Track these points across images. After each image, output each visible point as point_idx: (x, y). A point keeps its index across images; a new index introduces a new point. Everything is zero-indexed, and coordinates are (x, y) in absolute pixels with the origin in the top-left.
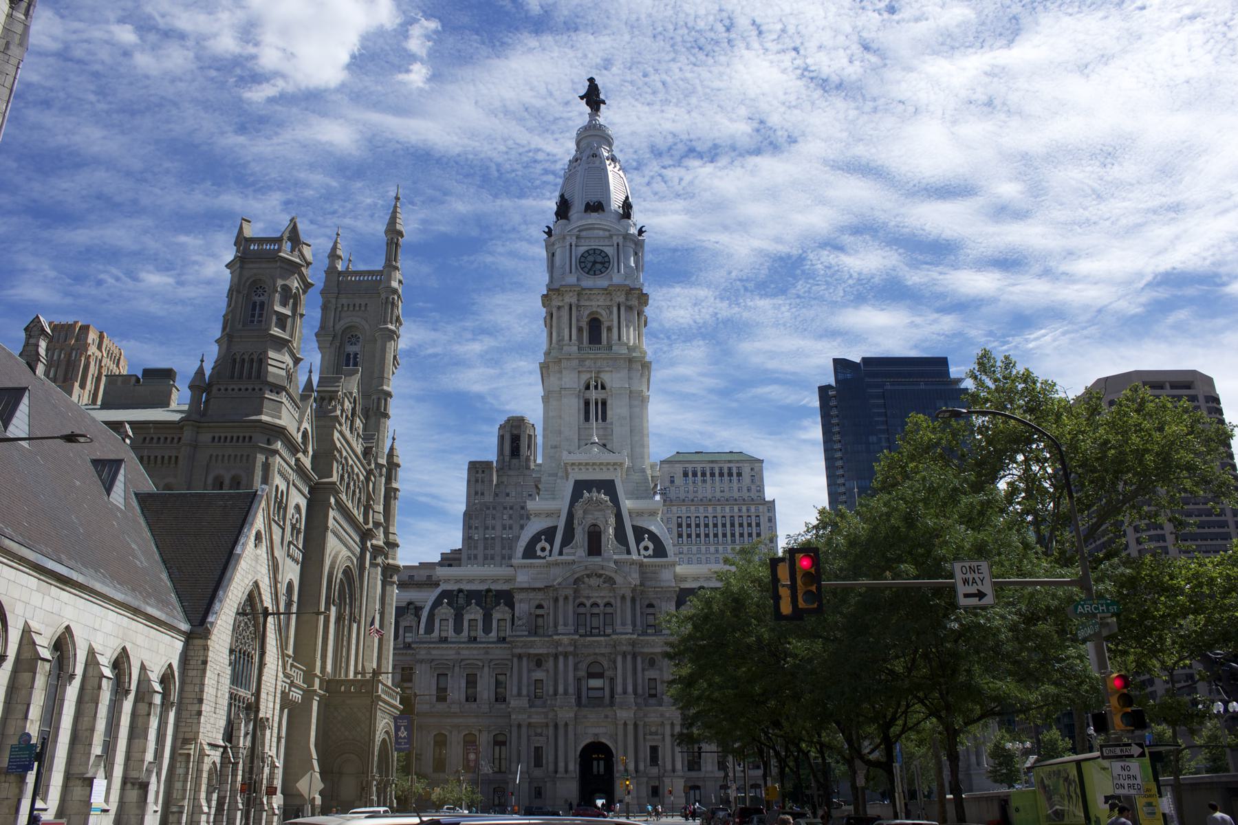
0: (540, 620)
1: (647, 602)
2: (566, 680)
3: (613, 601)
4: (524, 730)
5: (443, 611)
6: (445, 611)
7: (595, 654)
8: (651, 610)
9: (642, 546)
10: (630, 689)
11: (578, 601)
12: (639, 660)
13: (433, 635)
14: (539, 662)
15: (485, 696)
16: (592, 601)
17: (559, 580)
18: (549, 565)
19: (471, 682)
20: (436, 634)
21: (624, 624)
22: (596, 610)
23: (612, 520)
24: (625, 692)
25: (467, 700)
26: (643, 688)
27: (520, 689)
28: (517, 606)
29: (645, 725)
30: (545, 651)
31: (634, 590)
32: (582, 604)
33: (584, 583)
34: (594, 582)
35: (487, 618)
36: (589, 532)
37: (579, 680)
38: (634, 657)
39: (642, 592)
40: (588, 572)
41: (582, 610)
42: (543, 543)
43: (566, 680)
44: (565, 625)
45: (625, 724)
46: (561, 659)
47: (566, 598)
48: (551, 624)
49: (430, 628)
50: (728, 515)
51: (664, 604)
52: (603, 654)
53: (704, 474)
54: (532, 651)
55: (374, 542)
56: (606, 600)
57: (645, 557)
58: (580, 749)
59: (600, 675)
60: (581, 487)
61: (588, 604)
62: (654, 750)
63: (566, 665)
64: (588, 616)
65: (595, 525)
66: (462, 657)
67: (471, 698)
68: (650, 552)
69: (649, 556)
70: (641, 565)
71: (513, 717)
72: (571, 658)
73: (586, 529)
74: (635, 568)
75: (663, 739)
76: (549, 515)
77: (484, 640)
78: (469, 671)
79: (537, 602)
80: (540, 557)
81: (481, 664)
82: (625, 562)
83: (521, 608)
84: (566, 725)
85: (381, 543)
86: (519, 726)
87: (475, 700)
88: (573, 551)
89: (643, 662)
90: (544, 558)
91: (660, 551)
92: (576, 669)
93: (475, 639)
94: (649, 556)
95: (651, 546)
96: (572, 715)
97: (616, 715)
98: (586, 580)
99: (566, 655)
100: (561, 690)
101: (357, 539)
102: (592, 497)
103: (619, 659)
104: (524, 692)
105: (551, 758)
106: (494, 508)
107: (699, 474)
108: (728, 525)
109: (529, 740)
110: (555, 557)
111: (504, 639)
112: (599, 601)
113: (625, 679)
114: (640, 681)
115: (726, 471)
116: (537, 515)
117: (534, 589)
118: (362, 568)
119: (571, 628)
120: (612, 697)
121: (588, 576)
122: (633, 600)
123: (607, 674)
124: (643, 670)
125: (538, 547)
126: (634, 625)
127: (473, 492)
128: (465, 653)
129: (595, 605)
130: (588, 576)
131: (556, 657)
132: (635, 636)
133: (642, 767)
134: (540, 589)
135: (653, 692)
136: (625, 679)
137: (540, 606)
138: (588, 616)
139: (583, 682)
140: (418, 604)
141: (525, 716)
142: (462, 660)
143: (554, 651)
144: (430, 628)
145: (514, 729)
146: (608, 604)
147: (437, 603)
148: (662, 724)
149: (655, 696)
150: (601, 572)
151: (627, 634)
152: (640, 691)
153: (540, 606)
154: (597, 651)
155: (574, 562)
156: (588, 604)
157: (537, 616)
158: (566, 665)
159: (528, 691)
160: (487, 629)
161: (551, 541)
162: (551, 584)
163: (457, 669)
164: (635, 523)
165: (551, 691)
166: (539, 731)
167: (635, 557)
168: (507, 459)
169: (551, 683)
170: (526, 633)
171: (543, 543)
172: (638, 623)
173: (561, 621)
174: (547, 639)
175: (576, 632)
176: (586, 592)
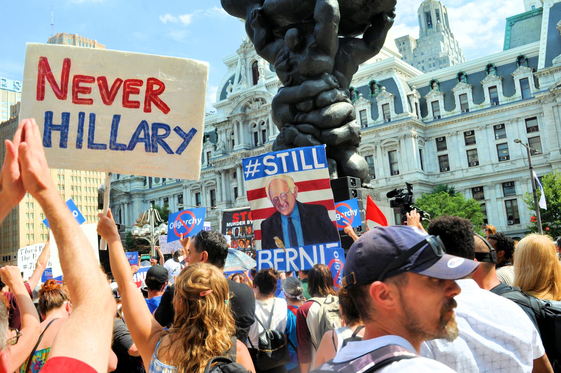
16: (259, 120)
33: (250, 108)
34: (255, 105)
36: (253, 68)
47: (238, 124)
54: (226, 167)
98: (250, 105)
104: (224, 198)
125: (228, 90)
161: (232, 83)
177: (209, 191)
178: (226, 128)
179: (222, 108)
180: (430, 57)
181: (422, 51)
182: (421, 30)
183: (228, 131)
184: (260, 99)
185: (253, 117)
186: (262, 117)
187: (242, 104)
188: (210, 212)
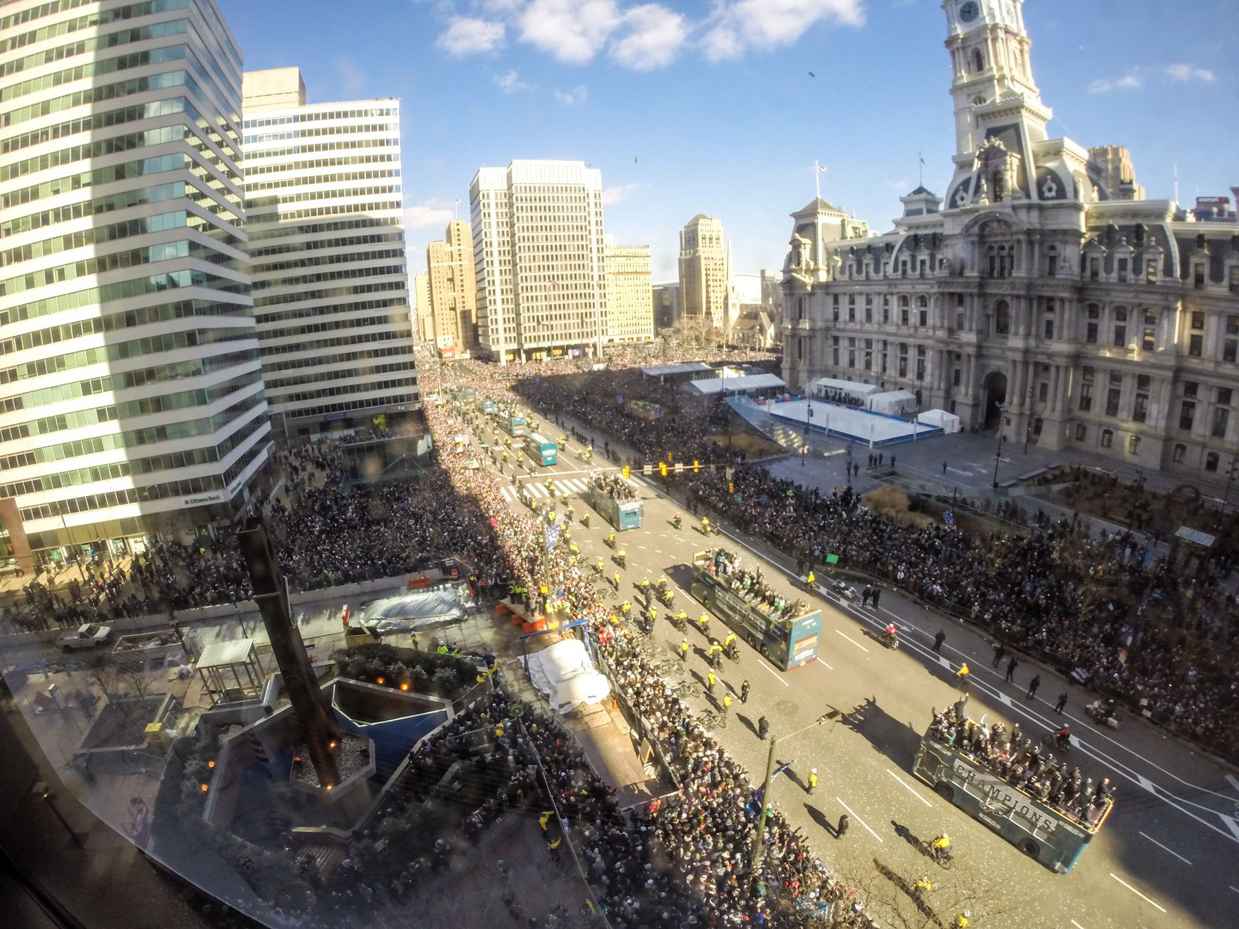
16: (999, 244)
29: (1037, 364)
32: (991, 248)
49: (896, 270)
54: (952, 290)
57: (1048, 199)
61: (996, 246)
68: (1053, 194)
69: (1052, 198)
94: (1052, 198)
95: (1054, 187)
112: (1004, 244)
122: (1031, 244)
155: (976, 210)
156: (996, 246)
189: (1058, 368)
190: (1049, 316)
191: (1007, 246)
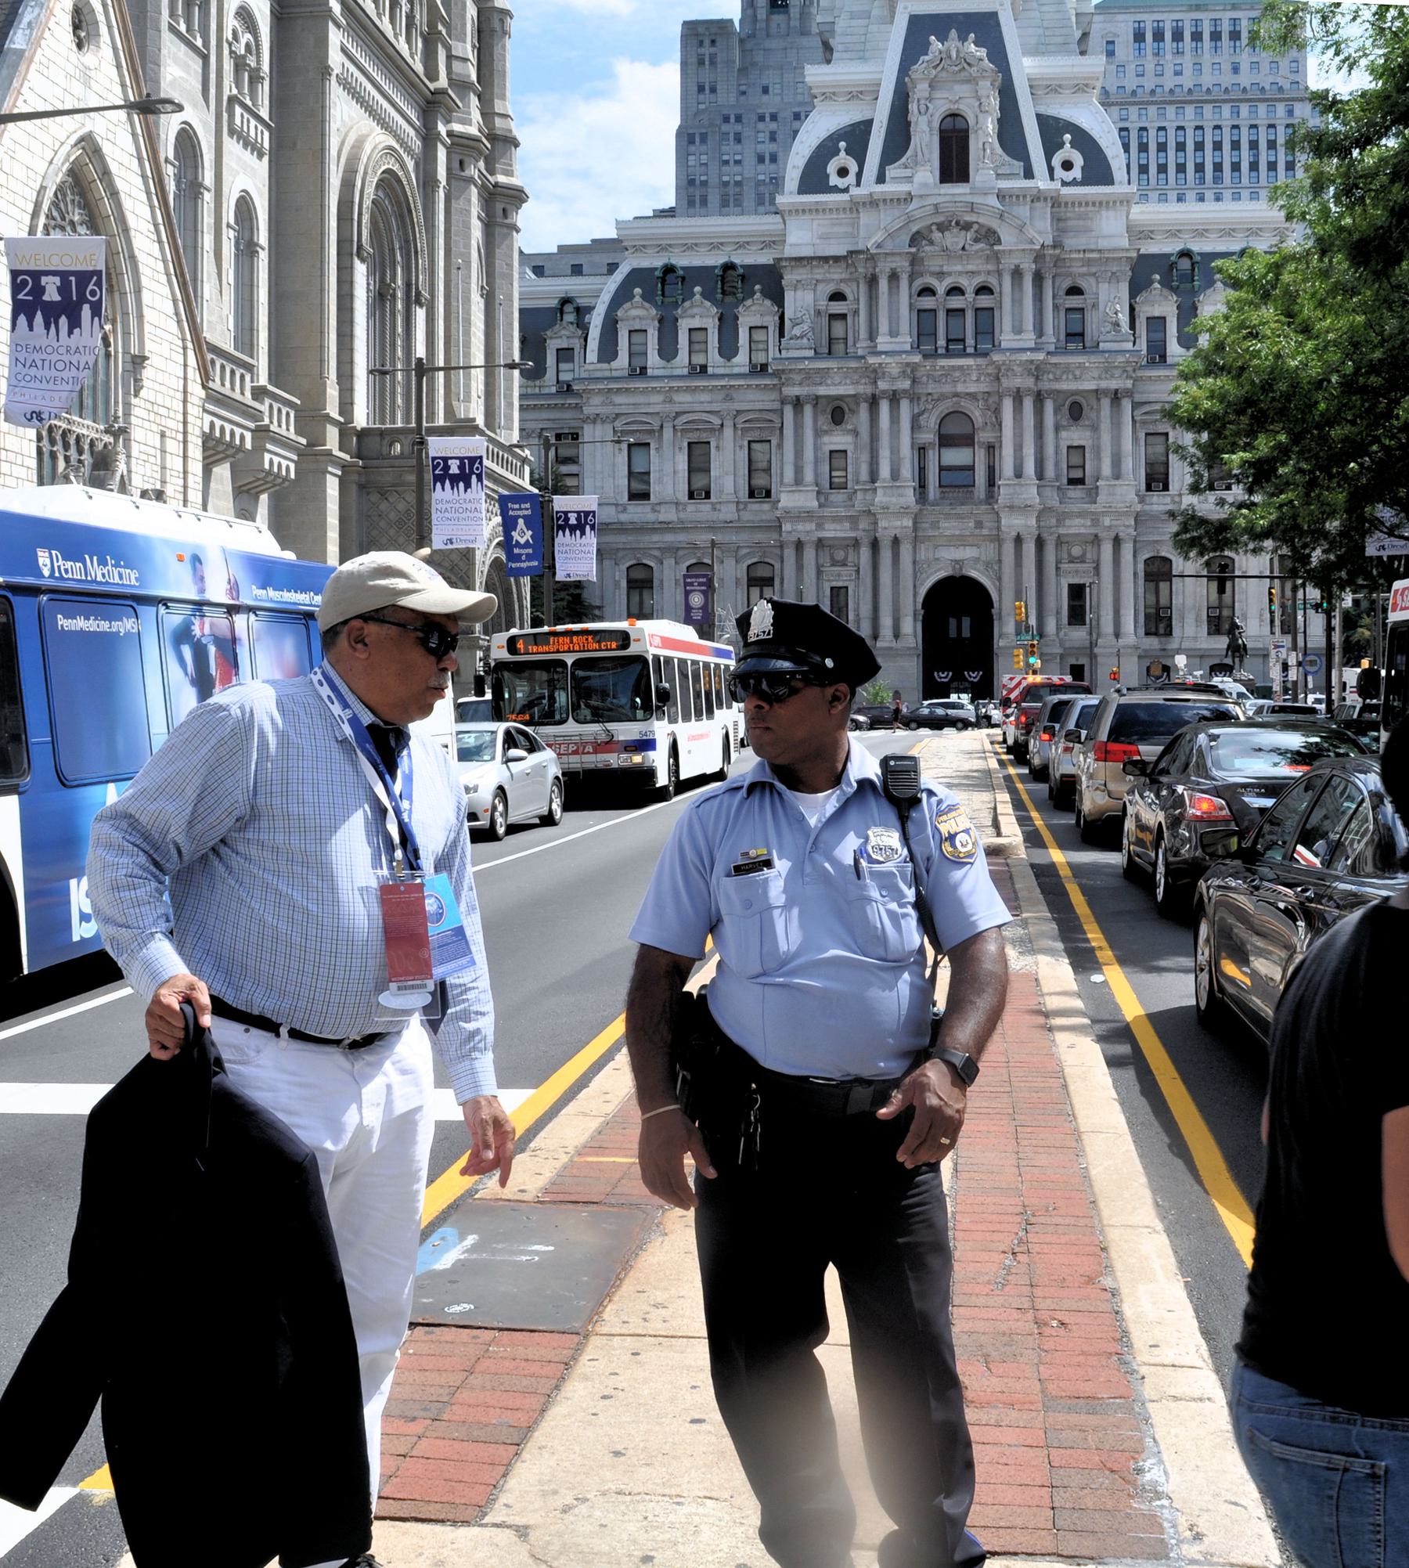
0: (838, 329)
1: (1067, 284)
2: (895, 451)
3: (993, 281)
4: (809, 554)
5: (634, 312)
6: (640, 313)
7: (956, 395)
8: (1074, 301)
9: (1056, 161)
10: (1030, 468)
11: (918, 284)
12: (1049, 407)
13: (614, 364)
14: (837, 413)
15: (728, 485)
16: (948, 282)
17: (878, 237)
18: (855, 206)
19: (698, 458)
20: (622, 361)
21: (1018, 330)
22: (956, 302)
23: (994, 102)
24: (1019, 474)
25: (691, 496)
26: (1057, 464)
27: (799, 471)
28: (789, 297)
29: (1060, 542)
30: (850, 390)
31: (1039, 257)
33: (931, 243)
34: (954, 239)
35: (727, 325)
36: (941, 131)
37: (922, 450)
38: (1039, 399)
39: (1058, 261)
40: (940, 219)
41: (928, 302)
42: (843, 159)
43: (895, 451)
44: (893, 333)
45: (1018, 540)
46: (884, 407)
47: (894, 277)
48: (863, 334)
49: (608, 351)
50: (1226, 124)
51: (1104, 287)
52: (973, 396)
53: (1178, 36)
54: (822, 391)
55: (457, 127)
56: (978, 281)
57: (1064, 184)
58: (923, 591)
59: (968, 441)
60: (922, 29)
61: (941, 288)
62: (1077, 592)
63: (895, 419)
64: (941, 316)
65: (954, 116)
66: (677, 408)
67: (699, 493)
68: (1076, 173)
69: (1074, 183)
70: (1056, 202)
71: (787, 527)
72: (905, 406)
73: (936, 124)
74: (1045, 211)
75: (1097, 569)
76: (855, 95)
77: (721, 371)
78: (694, 437)
79: (831, 288)
80: (836, 190)
81: (717, 421)
82: (1018, 197)
83: (800, 301)
84: (896, 541)
85: (473, 130)
86: (799, 546)
87: (708, 496)
88: (908, 173)
89: (1057, 411)
90: (846, 190)
91: (1097, 171)
92: (915, 426)
93: (704, 368)
94: (1074, 183)
95: (1078, 160)
96: (908, 523)
97: (999, 521)
98: (937, 235)
99: (894, 398)
100: (885, 471)
101: (412, 115)
102: (948, 51)
103: (1008, 405)
104: (809, 476)
105: (866, 610)
106: (739, 119)
107: (1168, 35)
108: (1227, 146)
109: (819, 573)
110: (869, 186)
111: (764, 367)
113: (1018, 448)
114: (1050, 450)
115: (1226, 28)
116: (829, 96)
117: (825, 259)
118: (428, 182)
119: (906, 340)
120: (991, 482)
121: (942, 228)
122: (1038, 278)
123: (984, 436)
124: (1057, 428)
125: (832, 168)
126: (1040, 332)
127: (693, 60)
128: (683, 400)
129: (956, 291)
130: (942, 228)
131: (873, 402)
132: (1041, 356)
133: (1051, 626)
134: (837, 259)
135: (1077, 474)
136: (1018, 448)
137: (838, 296)
138: (941, 316)
139: (932, 456)
140: (582, 302)
141: (813, 526)
142: (678, 414)
143: (869, 390)
144: (608, 351)
145: (789, 553)
146: (983, 290)
147: (622, 296)
148: (1096, 540)
149: (1080, 481)
150: (968, 218)
151: (1024, 350)
152: (1050, 472)
153: (838, 296)
154: (960, 388)
155: (909, 198)
156: (941, 288)
157: (833, 317)
158: (895, 419)
159: (816, 475)
160: (728, 350)
161: (859, 155)
162: (861, 247)
163: (668, 433)
164: (1043, 110)
165: (864, 475)
166: (840, 555)
167: (1042, 182)
168: (762, 14)
169: (865, 457)
170: (811, 353)
171: (843, 159)
172: (1049, 329)
173: (883, 325)
174: (853, 364)
175: (917, 347)
176: (933, 264)
177: (686, 444)
178: (818, 277)
179: (807, 216)
180: (797, 110)
181: (765, 82)
182: (750, 12)
183: (820, 287)
184: (976, 227)
185: (937, 269)
186: (960, 273)
187: (915, 228)
188: (685, 505)
189: (1117, 541)
190: (1076, 435)
191: (969, 285)
